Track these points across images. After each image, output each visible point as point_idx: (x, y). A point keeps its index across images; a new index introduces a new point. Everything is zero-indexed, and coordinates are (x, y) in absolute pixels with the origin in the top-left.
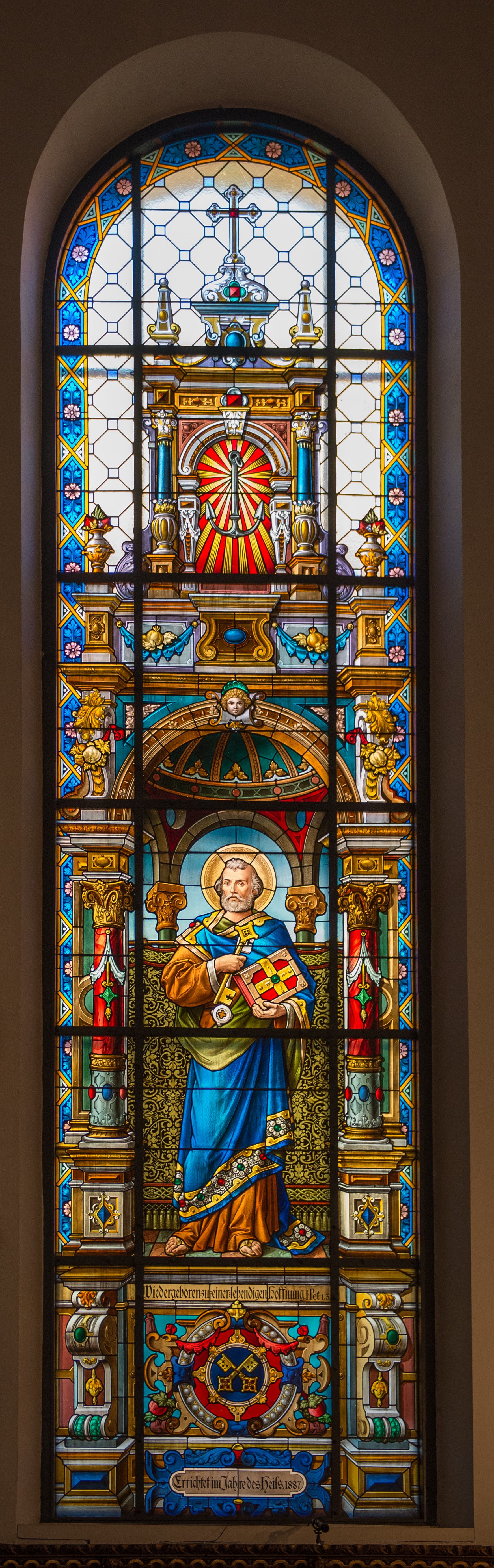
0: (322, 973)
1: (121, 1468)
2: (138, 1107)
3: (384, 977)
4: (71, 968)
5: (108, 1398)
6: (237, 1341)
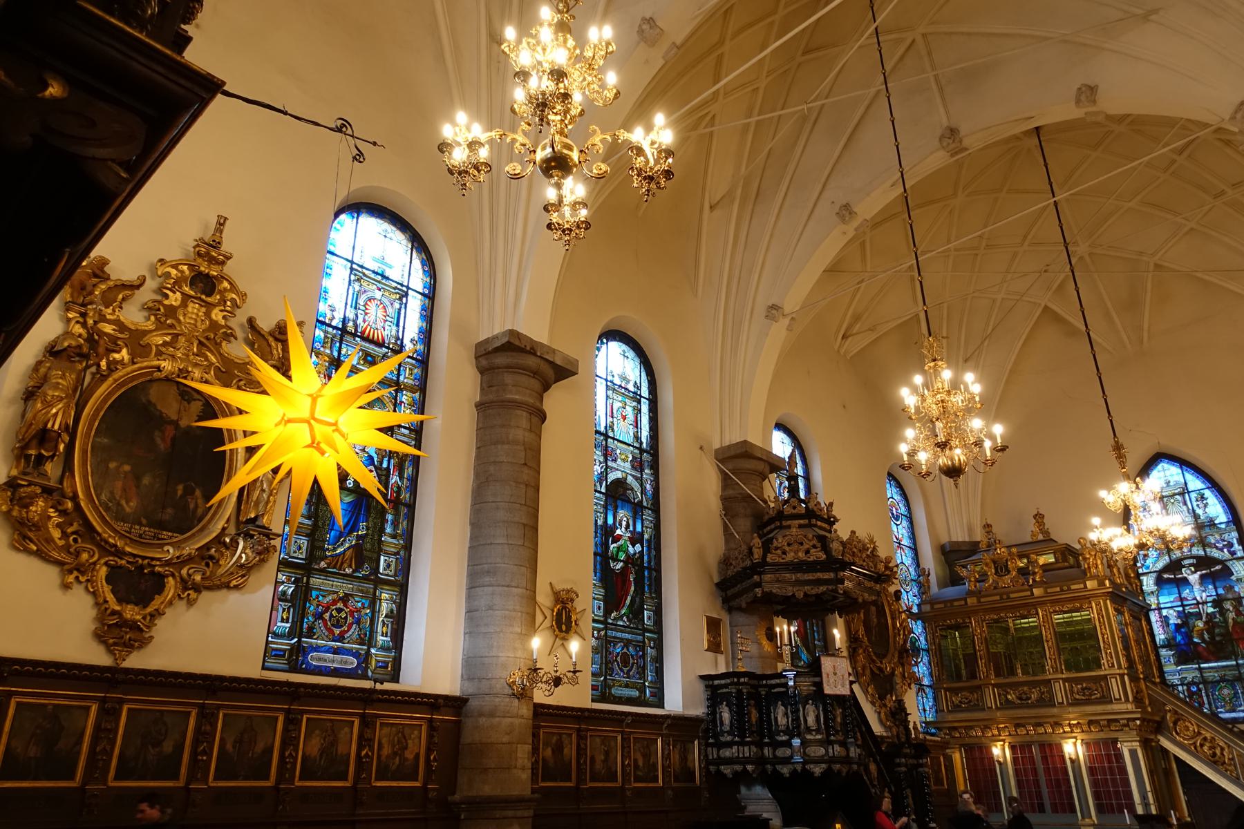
0: (384, 478)
1: (291, 651)
2: (316, 510)
3: (403, 484)
5: (290, 620)
6: (340, 605)
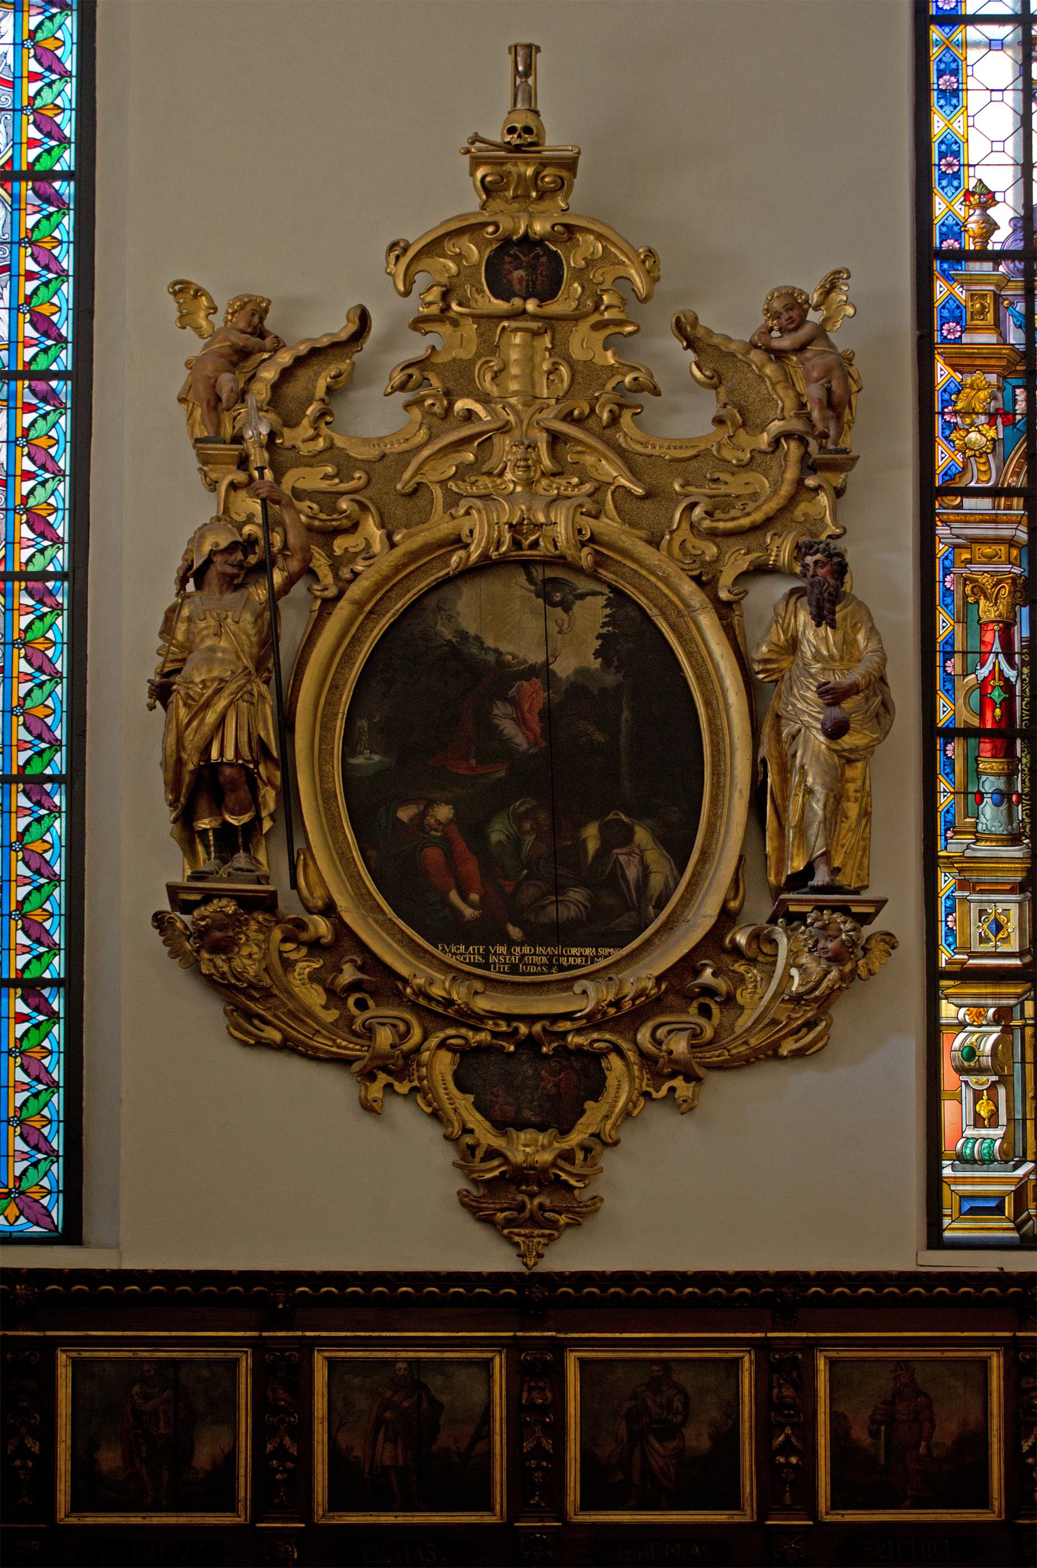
4: (955, 665)
5: (1003, 1119)
